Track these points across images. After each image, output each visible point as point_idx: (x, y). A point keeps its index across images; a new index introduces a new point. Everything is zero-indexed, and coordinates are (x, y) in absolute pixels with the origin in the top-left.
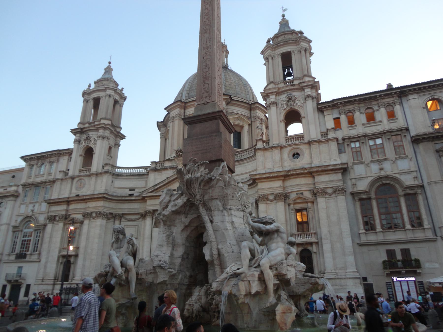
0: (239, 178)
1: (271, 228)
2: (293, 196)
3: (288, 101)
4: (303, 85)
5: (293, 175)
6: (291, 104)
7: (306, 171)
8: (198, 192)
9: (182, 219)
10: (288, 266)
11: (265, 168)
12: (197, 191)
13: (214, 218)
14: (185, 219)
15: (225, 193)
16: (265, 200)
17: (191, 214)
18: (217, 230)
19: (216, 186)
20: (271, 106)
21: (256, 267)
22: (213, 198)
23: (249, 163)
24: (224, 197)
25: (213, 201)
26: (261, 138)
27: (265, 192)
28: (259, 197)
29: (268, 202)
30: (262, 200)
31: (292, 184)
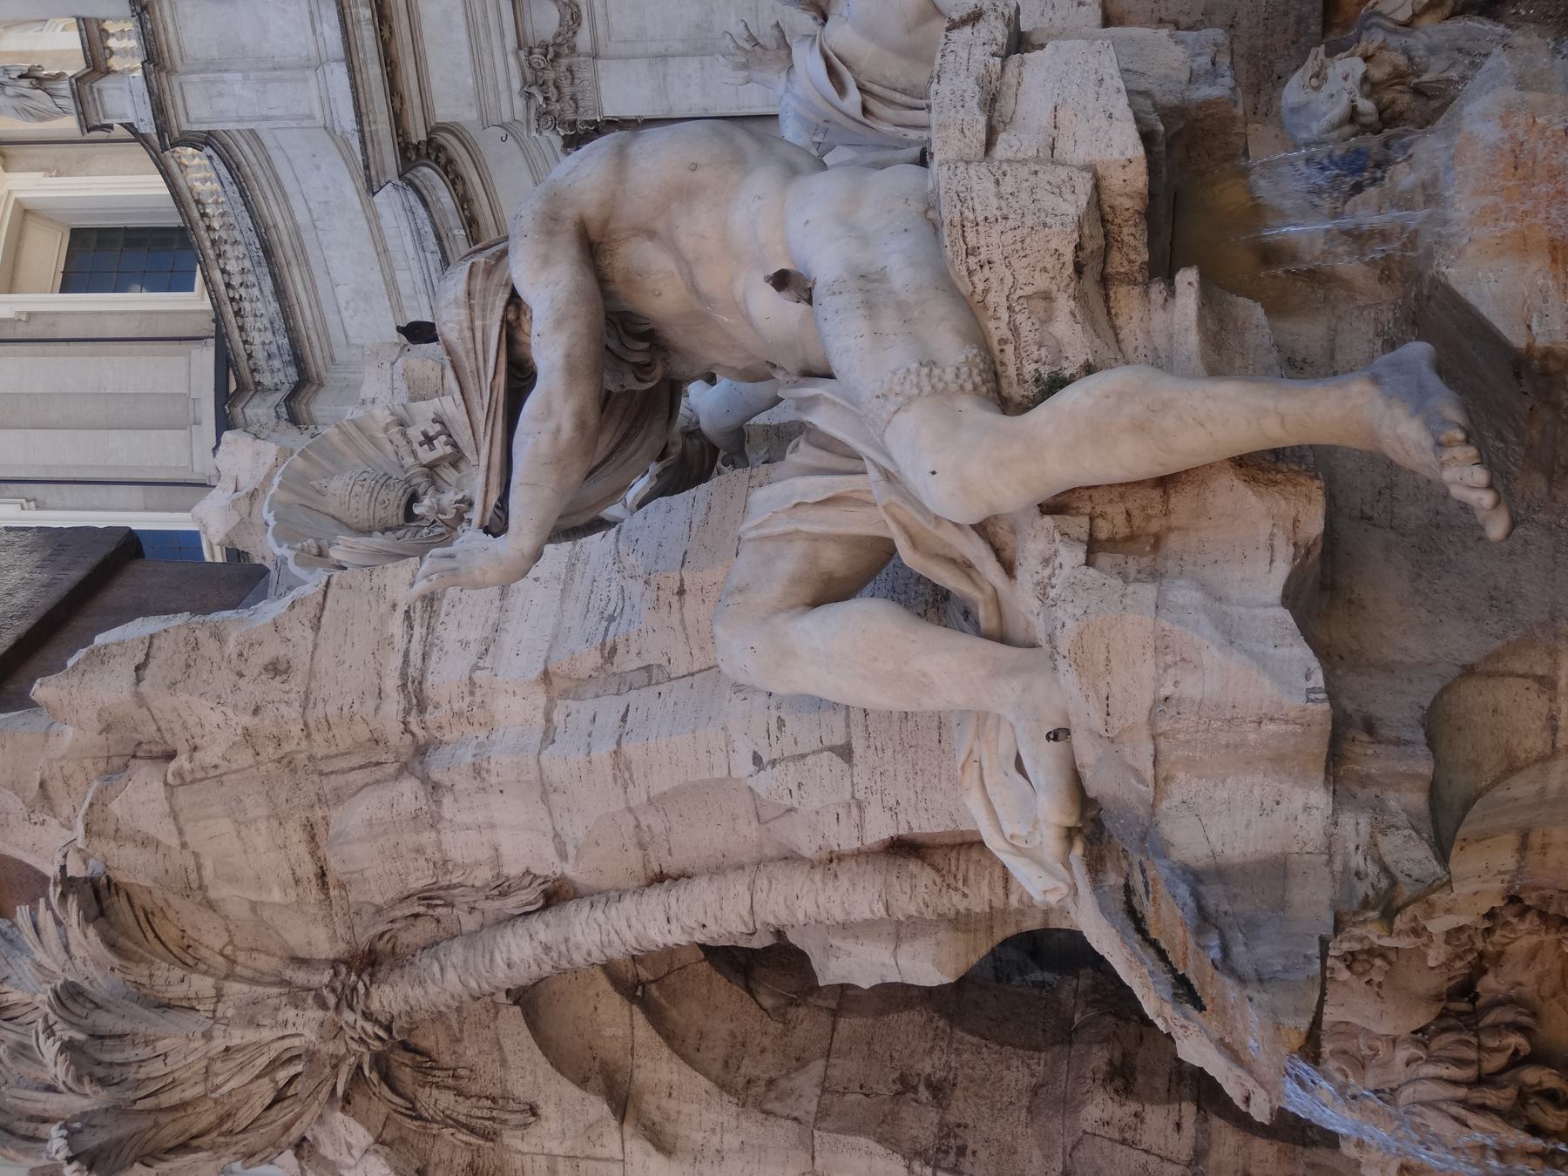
0: (415, 265)
1: (558, 324)
8: (254, 1023)
9: (551, 1157)
10: (1000, 150)
11: (319, 64)
12: (238, 1037)
15: (244, 758)
16: (570, 70)
17: (504, 1062)
18: (642, 846)
19: (174, 842)
21: (1009, 568)
22: (308, 869)
23: (290, 187)
24: (287, 762)
25: (335, 868)
26: (64, 87)
29: (583, 40)
30: (567, 90)
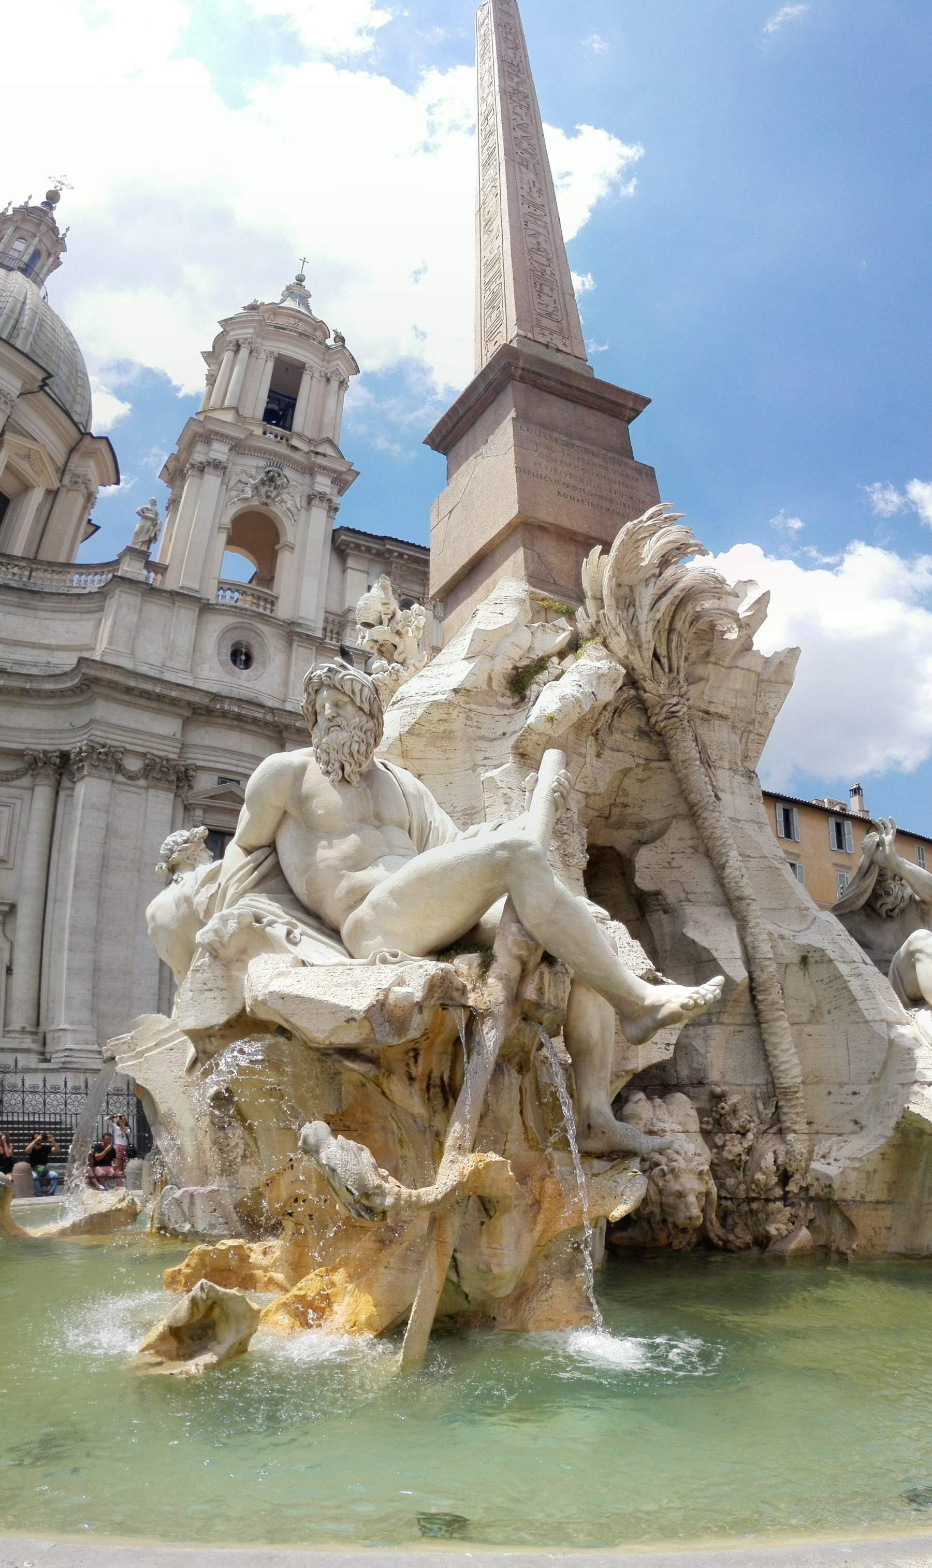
2: (205, 783)
3: (263, 483)
4: (320, 460)
5: (225, 714)
6: (269, 493)
7: (269, 718)
13: (720, 794)
14: (595, 762)
16: (109, 769)
17: (612, 749)
20: (206, 469)
22: (712, 709)
24: (752, 722)
27: (116, 739)
28: (81, 749)
29: (120, 778)
31: (217, 745)
